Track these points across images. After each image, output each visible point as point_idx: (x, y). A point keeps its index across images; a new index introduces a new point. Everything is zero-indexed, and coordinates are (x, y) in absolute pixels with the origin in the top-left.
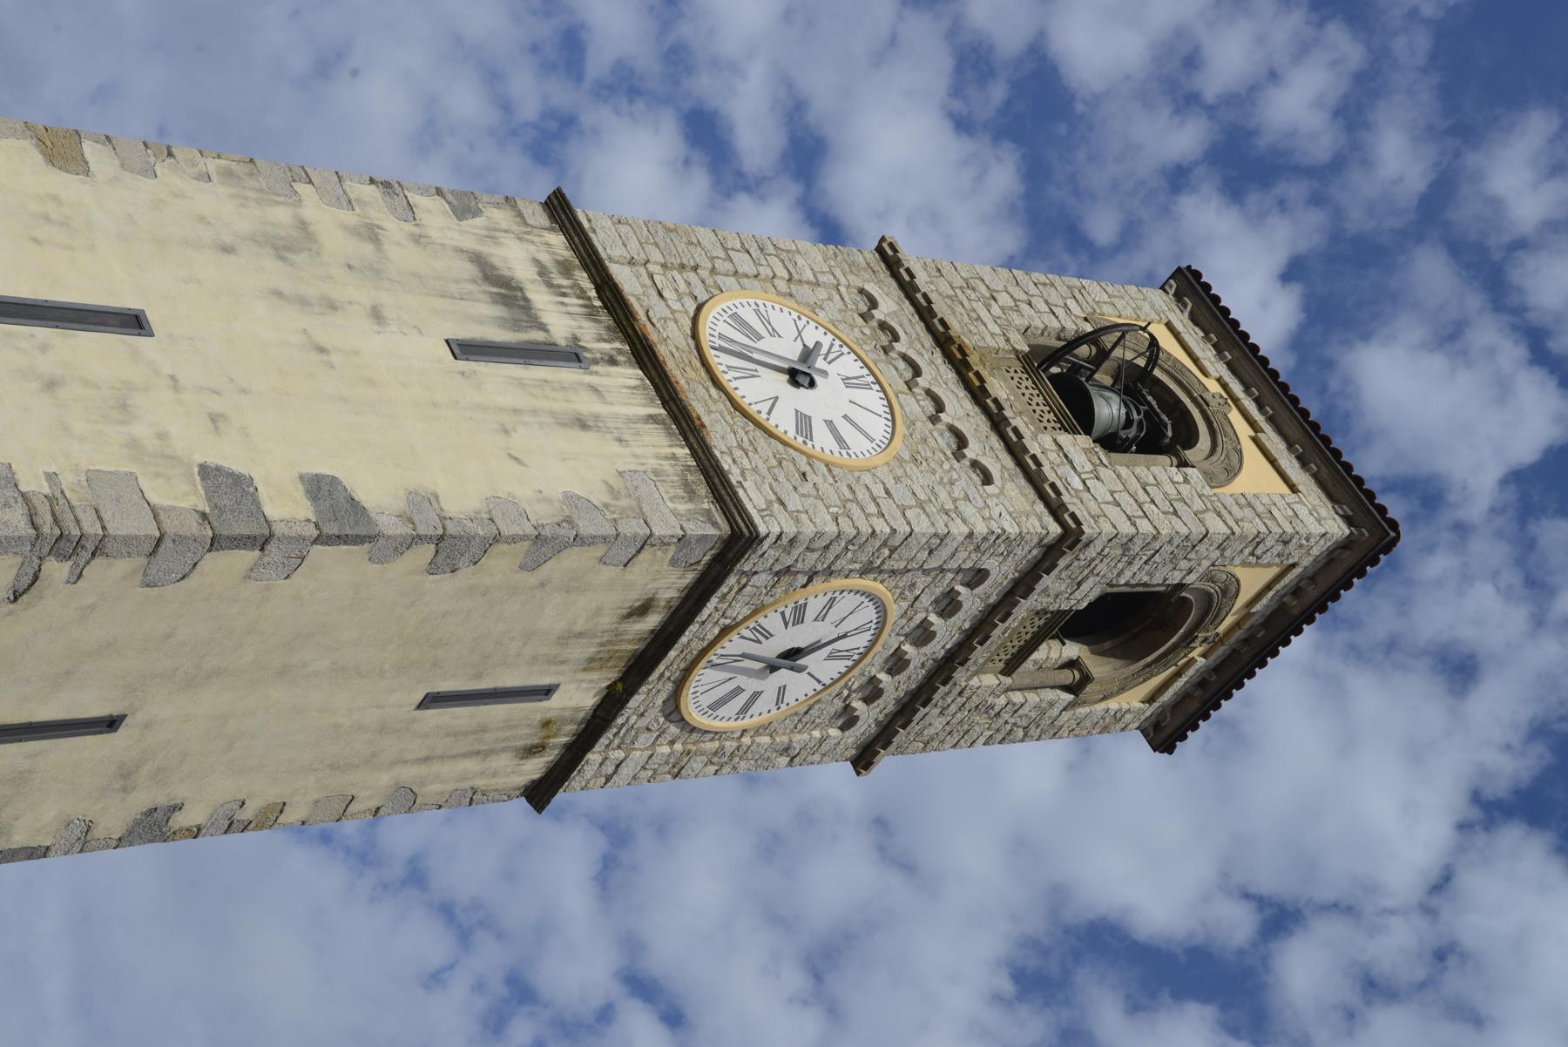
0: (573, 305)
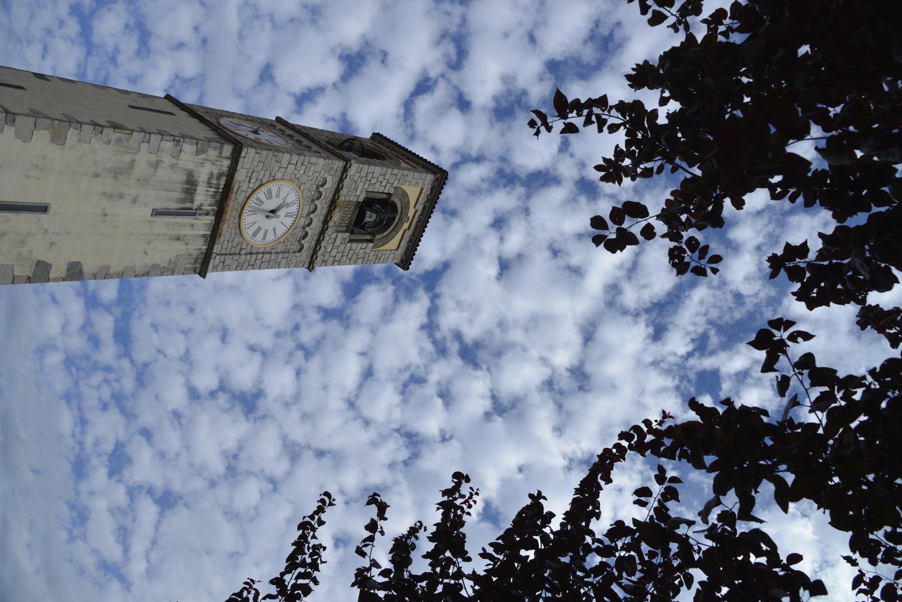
0: (211, 191)
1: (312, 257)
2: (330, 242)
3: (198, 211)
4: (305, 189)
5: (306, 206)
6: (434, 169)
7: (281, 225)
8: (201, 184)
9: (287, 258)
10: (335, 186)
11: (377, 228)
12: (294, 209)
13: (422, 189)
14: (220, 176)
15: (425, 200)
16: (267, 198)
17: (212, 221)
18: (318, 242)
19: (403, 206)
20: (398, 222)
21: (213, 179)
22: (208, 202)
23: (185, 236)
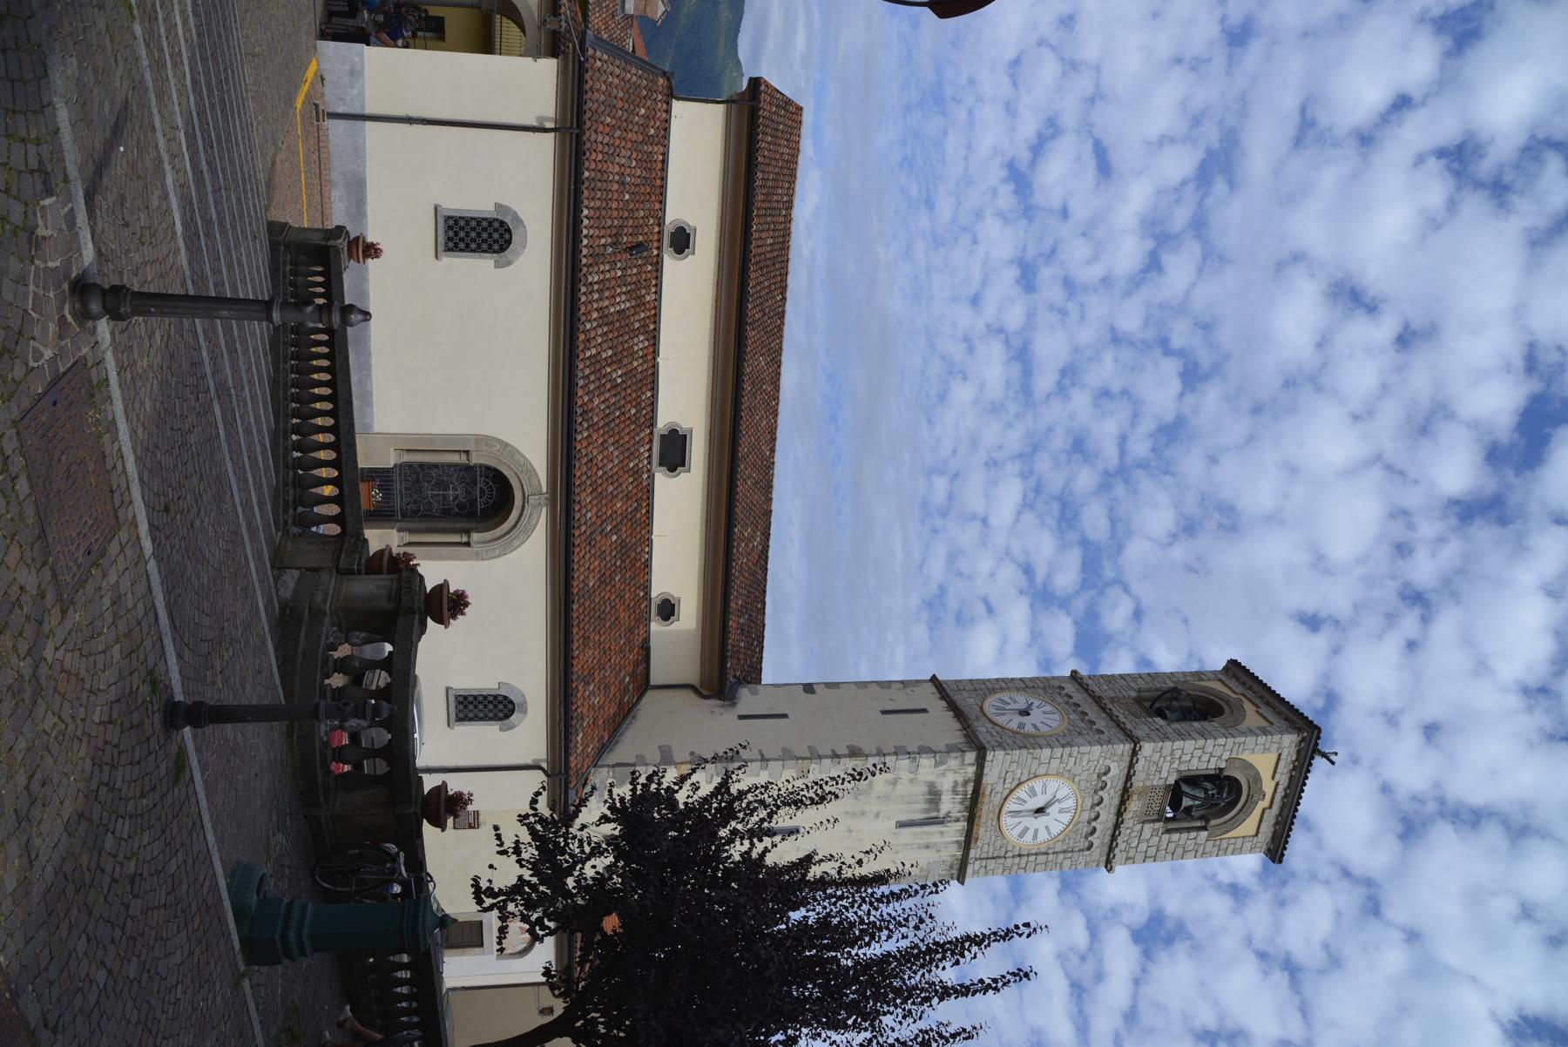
1: (1109, 855)
6: (1300, 723)
7: (1055, 823)
10: (1126, 772)
11: (1212, 810)
12: (1070, 803)
13: (1280, 755)
14: (966, 783)
18: (1114, 838)
20: (1247, 801)
22: (957, 810)
23: (935, 844)
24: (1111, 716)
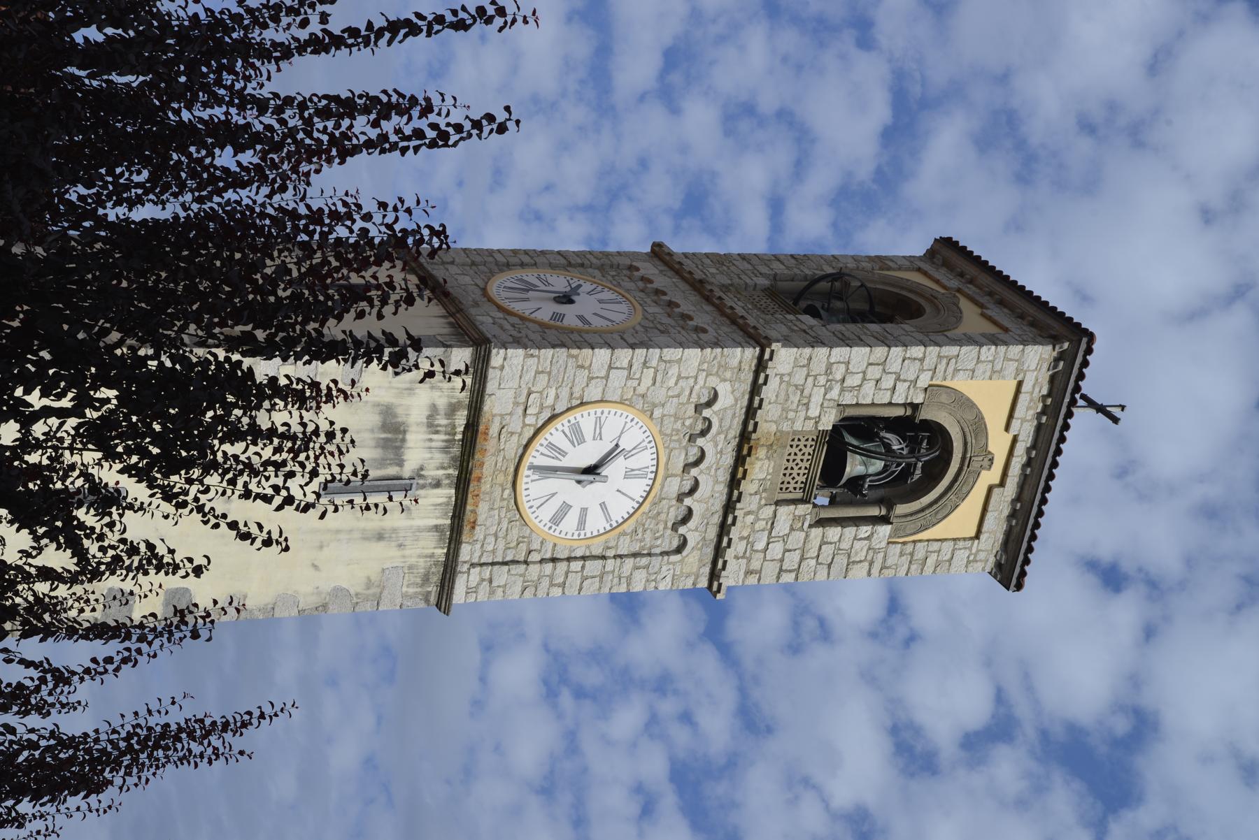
0: (437, 441)
1: (714, 563)
2: (757, 526)
3: (414, 482)
4: (664, 416)
5: (676, 452)
6: (1057, 327)
8: (413, 428)
9: (647, 567)
10: (745, 402)
12: (645, 459)
13: (1020, 384)
14: (452, 409)
15: (1039, 410)
16: (573, 443)
17: (450, 498)
18: (723, 529)
19: (966, 430)
21: (438, 417)
23: (394, 530)
24: (720, 308)
